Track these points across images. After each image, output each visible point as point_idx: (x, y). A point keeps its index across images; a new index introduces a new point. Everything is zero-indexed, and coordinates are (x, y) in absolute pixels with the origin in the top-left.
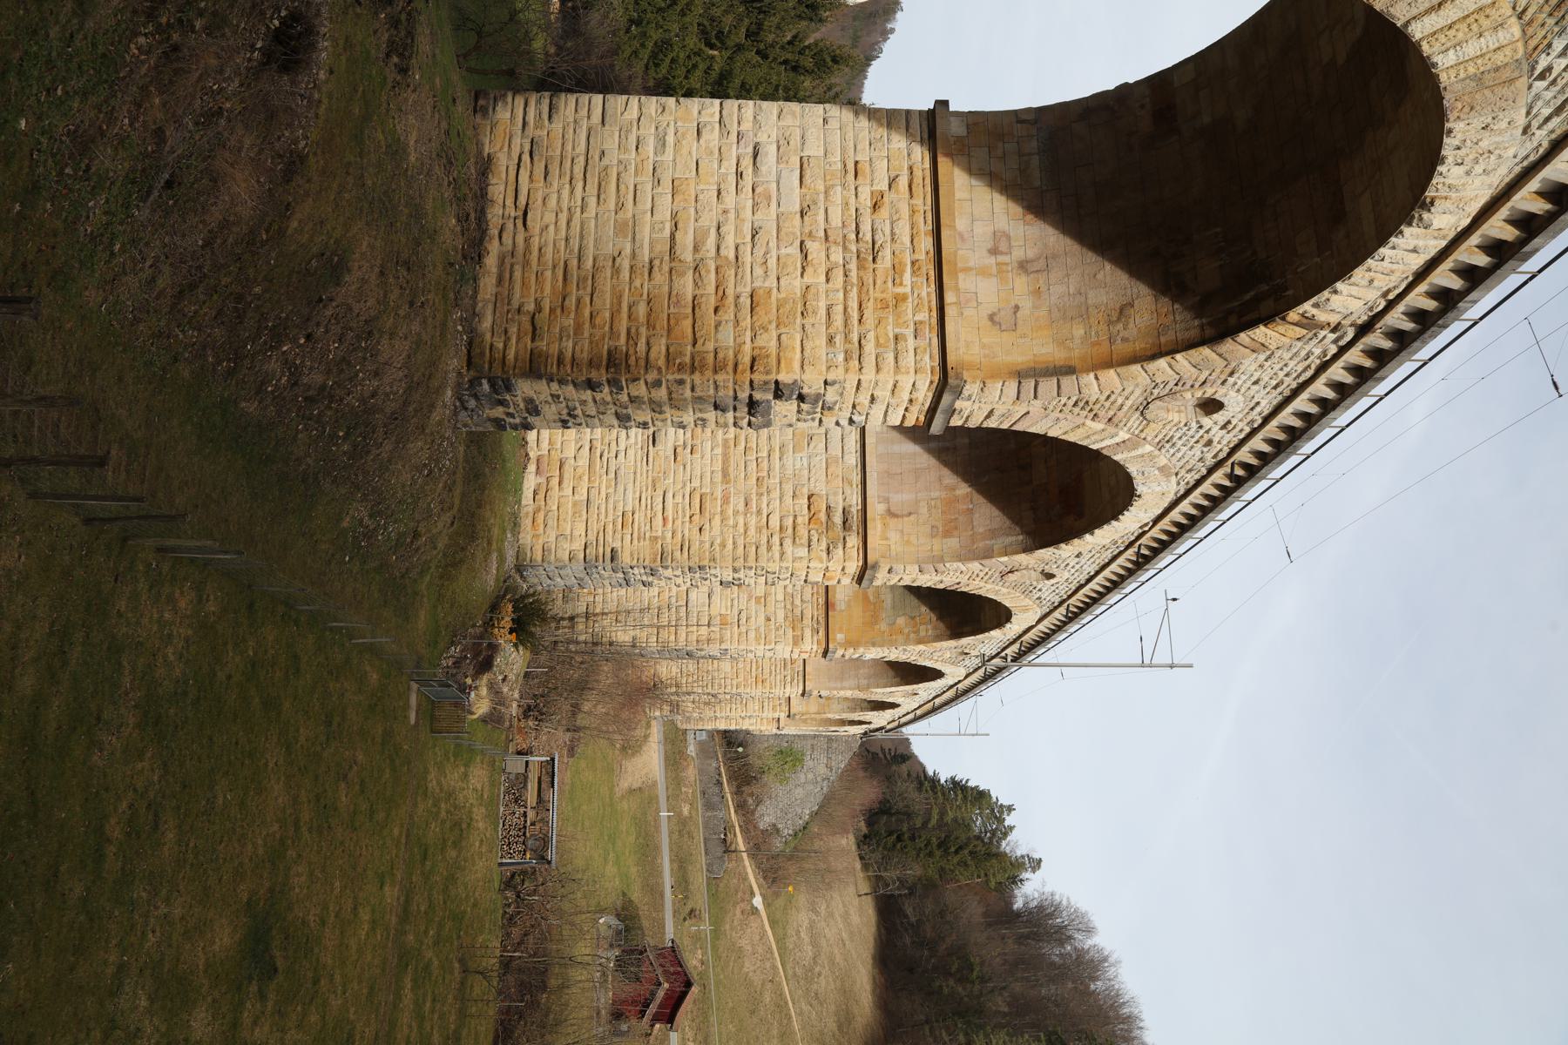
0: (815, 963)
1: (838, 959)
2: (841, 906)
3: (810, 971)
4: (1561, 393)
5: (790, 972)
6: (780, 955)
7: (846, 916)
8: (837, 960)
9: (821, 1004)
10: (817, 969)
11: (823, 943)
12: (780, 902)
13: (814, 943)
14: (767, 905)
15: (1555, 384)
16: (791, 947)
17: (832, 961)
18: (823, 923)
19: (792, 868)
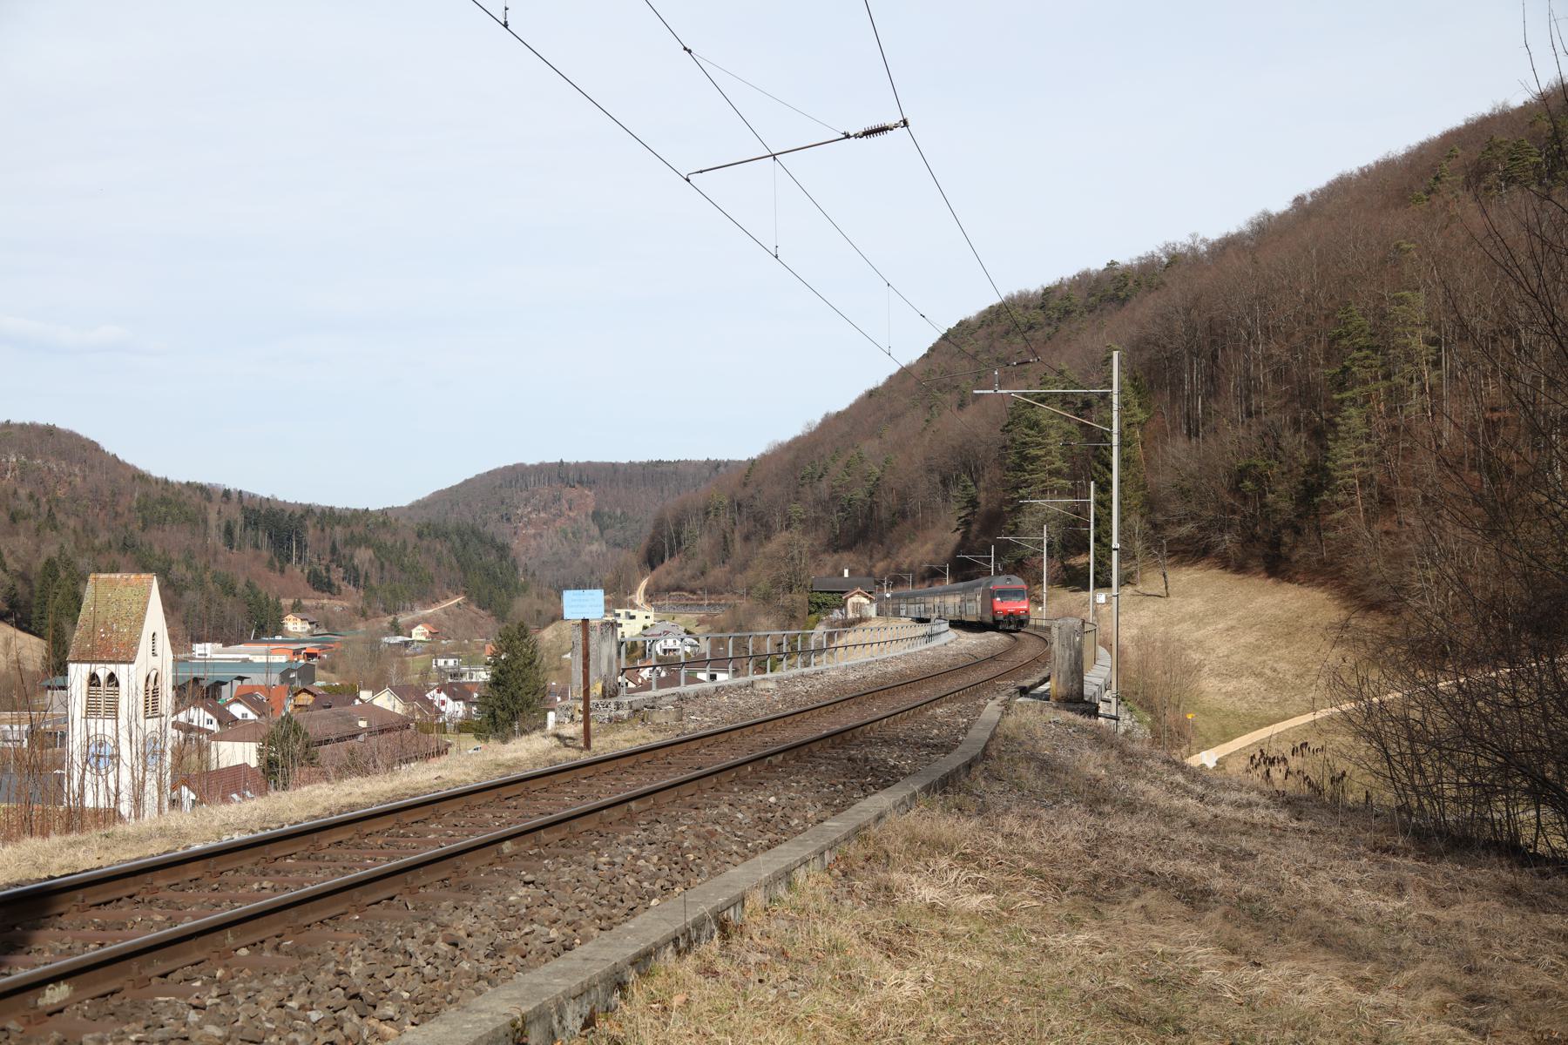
0: (1260, 675)
1: (1250, 638)
2: (1185, 626)
3: (1271, 682)
4: (898, 119)
5: (1276, 710)
6: (1260, 726)
7: (1199, 620)
8: (1252, 640)
9: (1309, 670)
10: (1268, 672)
11: (1236, 659)
12: (1203, 724)
13: (1237, 672)
14: (1207, 744)
15: (867, 133)
16: (1246, 705)
17: (1256, 648)
18: (1212, 657)
19: (1170, 717)
